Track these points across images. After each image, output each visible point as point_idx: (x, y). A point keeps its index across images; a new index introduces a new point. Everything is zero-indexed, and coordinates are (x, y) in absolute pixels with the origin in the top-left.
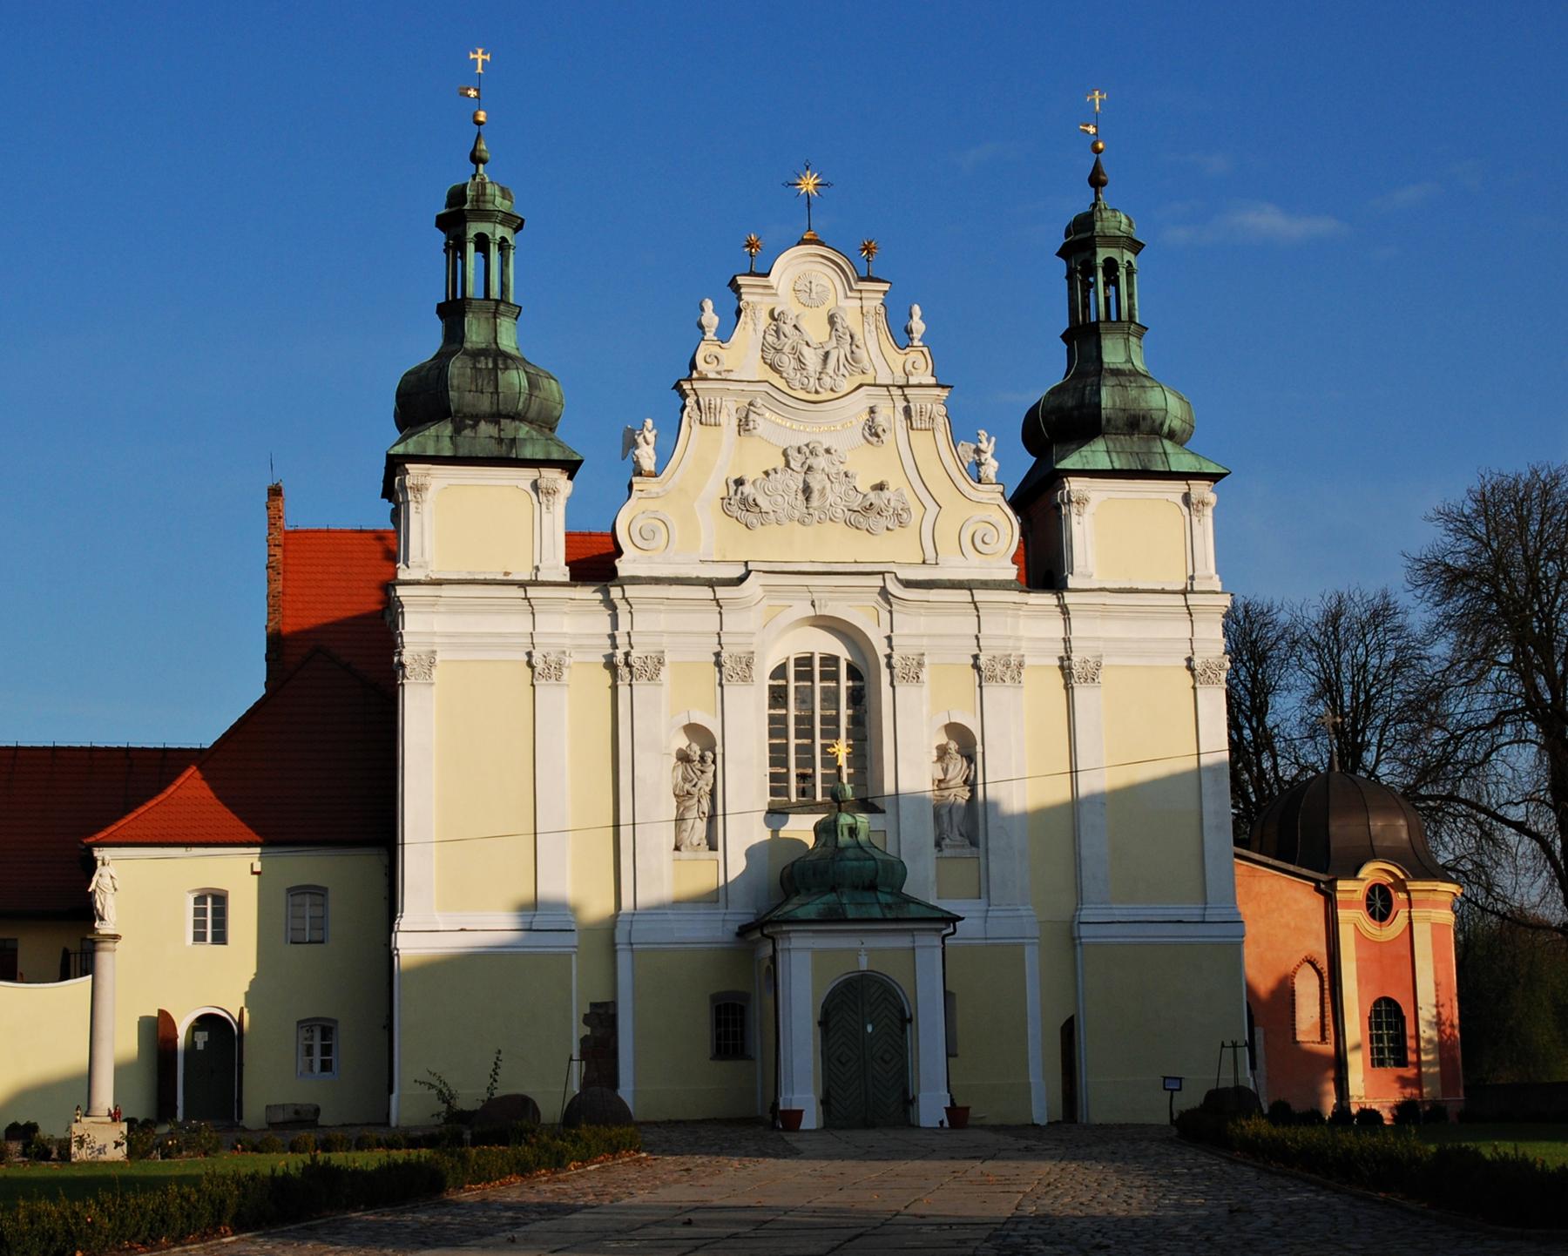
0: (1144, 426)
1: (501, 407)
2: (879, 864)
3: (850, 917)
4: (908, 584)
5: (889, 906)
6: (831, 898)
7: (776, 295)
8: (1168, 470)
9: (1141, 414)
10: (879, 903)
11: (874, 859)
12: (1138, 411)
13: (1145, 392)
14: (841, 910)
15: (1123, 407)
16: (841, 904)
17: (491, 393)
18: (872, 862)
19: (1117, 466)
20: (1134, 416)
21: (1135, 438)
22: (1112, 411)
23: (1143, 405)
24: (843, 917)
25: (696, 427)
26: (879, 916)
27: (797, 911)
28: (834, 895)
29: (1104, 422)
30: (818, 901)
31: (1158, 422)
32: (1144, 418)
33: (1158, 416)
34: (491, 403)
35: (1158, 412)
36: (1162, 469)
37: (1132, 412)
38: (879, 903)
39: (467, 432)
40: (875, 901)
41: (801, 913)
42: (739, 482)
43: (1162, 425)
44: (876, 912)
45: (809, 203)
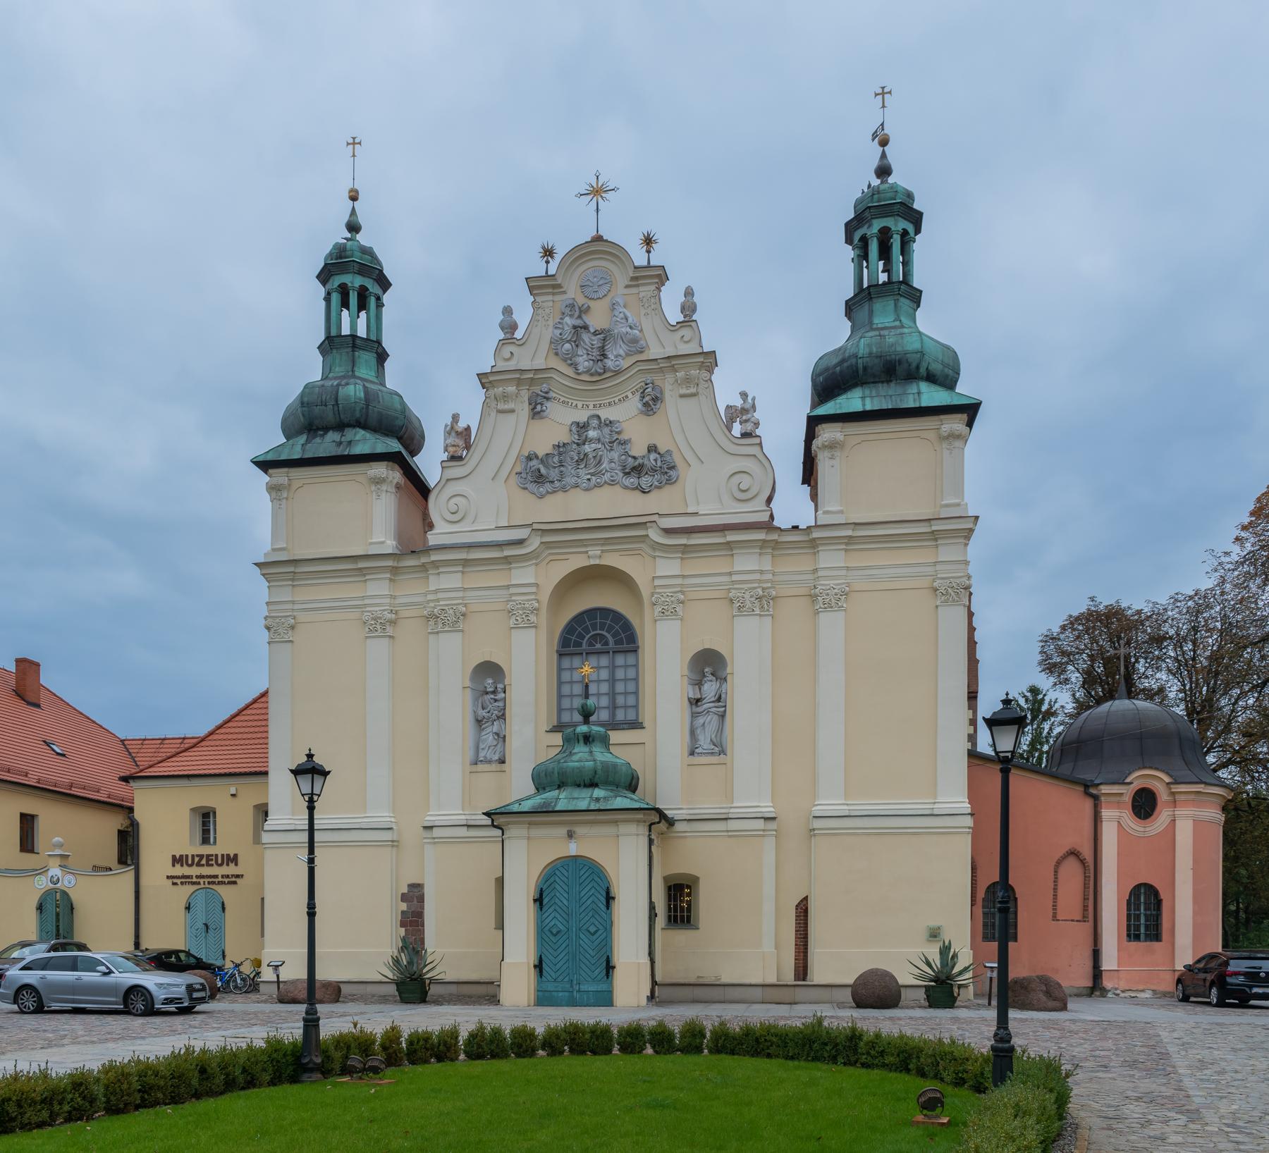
0: (900, 370)
1: (342, 416)
4: (669, 532)
7: (564, 292)
8: (917, 405)
9: (897, 358)
12: (893, 357)
13: (902, 338)
15: (879, 354)
17: (333, 405)
19: (868, 407)
20: (890, 361)
21: (892, 384)
22: (868, 359)
23: (899, 349)
25: (493, 414)
29: (861, 372)
31: (914, 365)
32: (900, 362)
33: (913, 359)
34: (334, 414)
35: (915, 355)
36: (913, 406)
37: (888, 358)
39: (318, 440)
42: (529, 458)
43: (918, 367)
45: (597, 209)
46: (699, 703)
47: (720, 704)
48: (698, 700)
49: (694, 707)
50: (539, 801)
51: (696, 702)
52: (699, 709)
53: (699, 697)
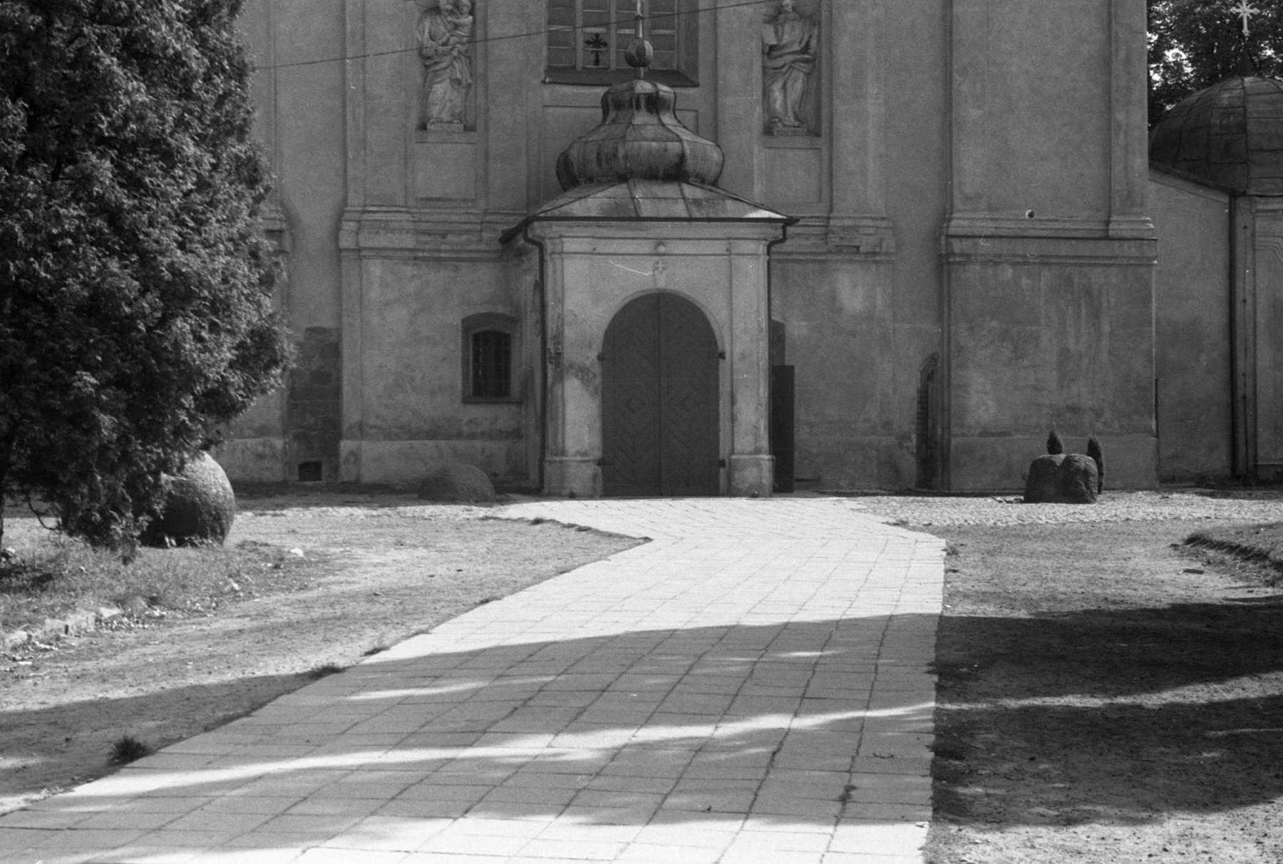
2: (686, 146)
3: (645, 214)
5: (697, 203)
6: (619, 191)
10: (684, 198)
11: (680, 140)
14: (632, 207)
16: (633, 198)
18: (677, 144)
24: (634, 215)
26: (685, 215)
27: (571, 205)
28: (624, 186)
30: (599, 195)
38: (684, 198)
40: (678, 195)
41: (577, 209)
44: (680, 210)
46: (775, 54)
47: (806, 56)
48: (772, 48)
49: (766, 58)
50: (606, 200)
51: (770, 51)
52: (779, 62)
53: (774, 43)
